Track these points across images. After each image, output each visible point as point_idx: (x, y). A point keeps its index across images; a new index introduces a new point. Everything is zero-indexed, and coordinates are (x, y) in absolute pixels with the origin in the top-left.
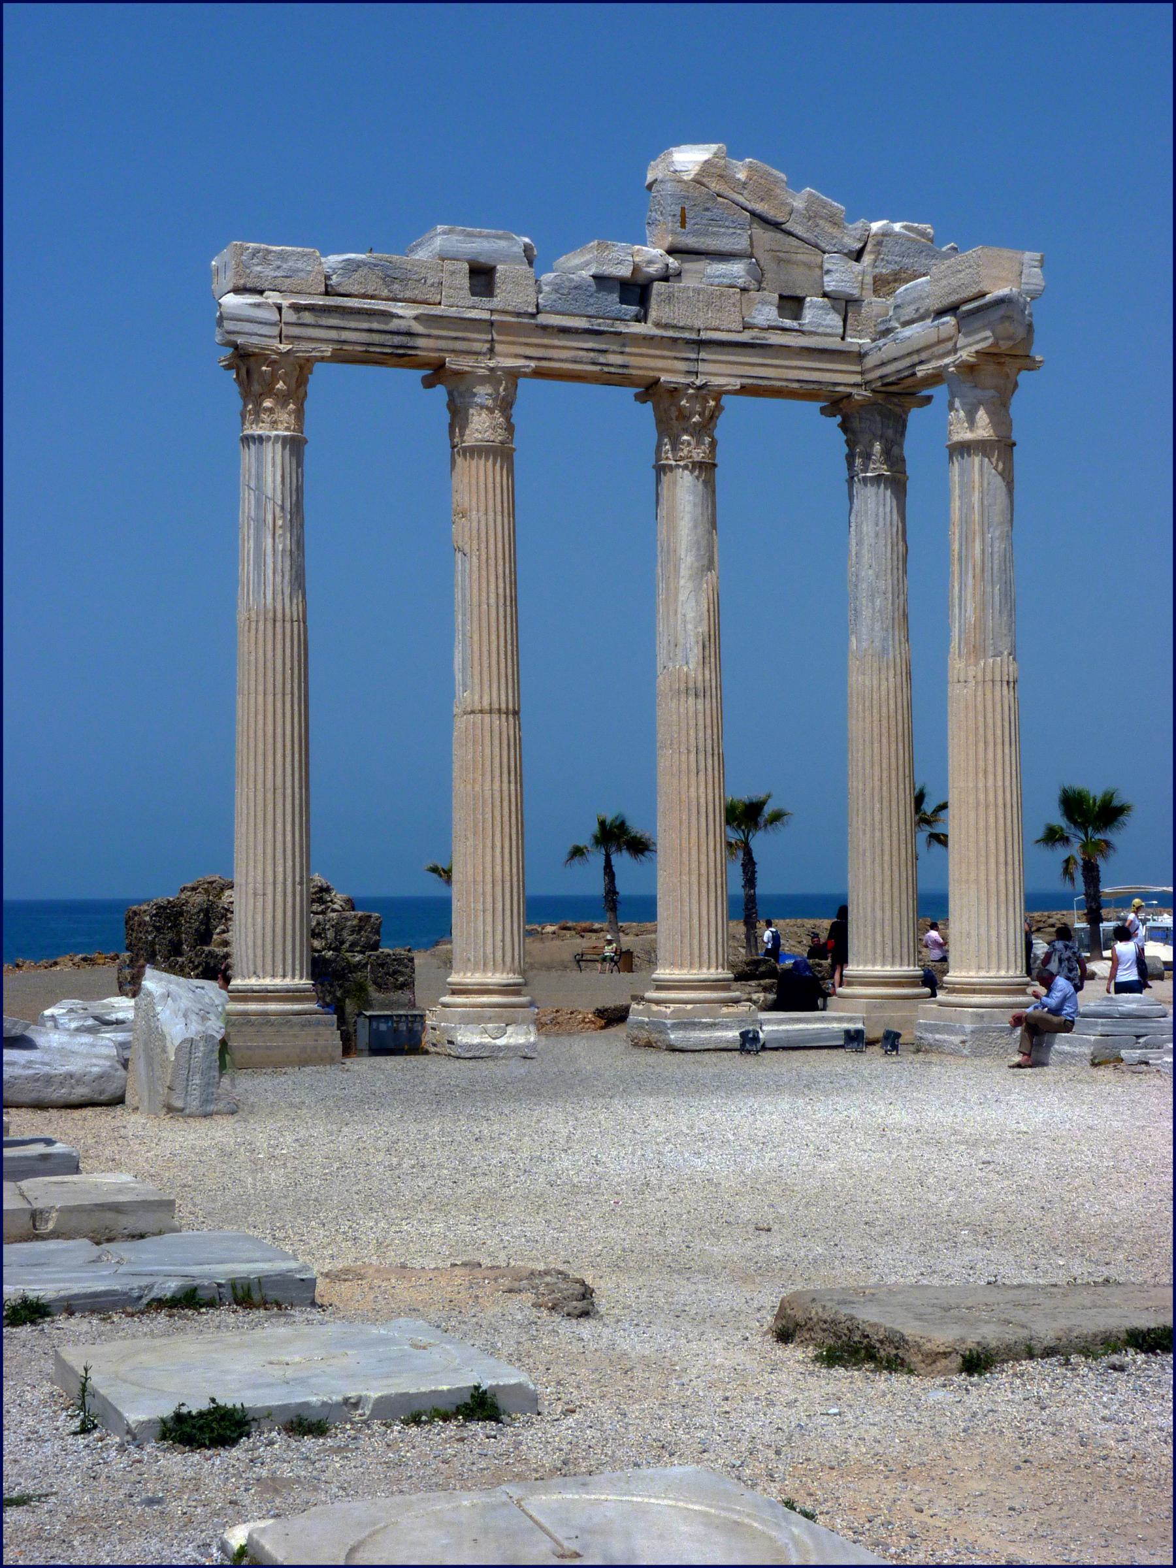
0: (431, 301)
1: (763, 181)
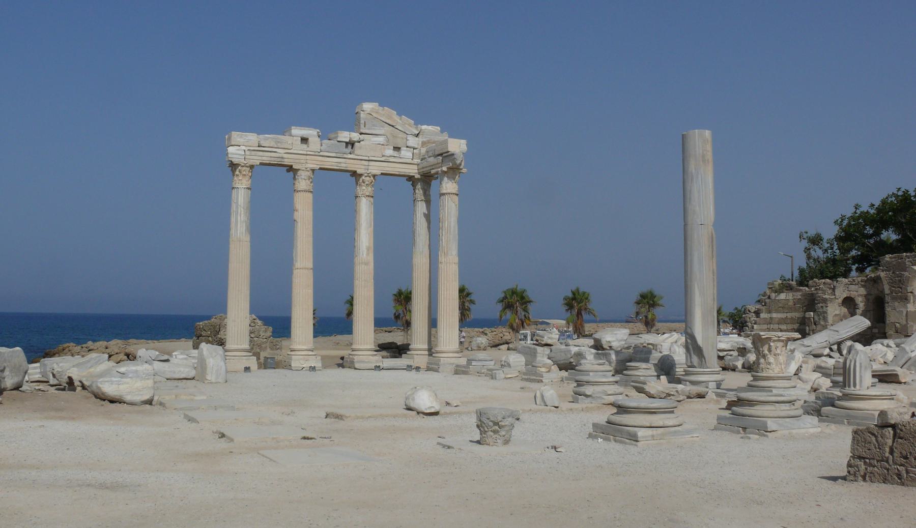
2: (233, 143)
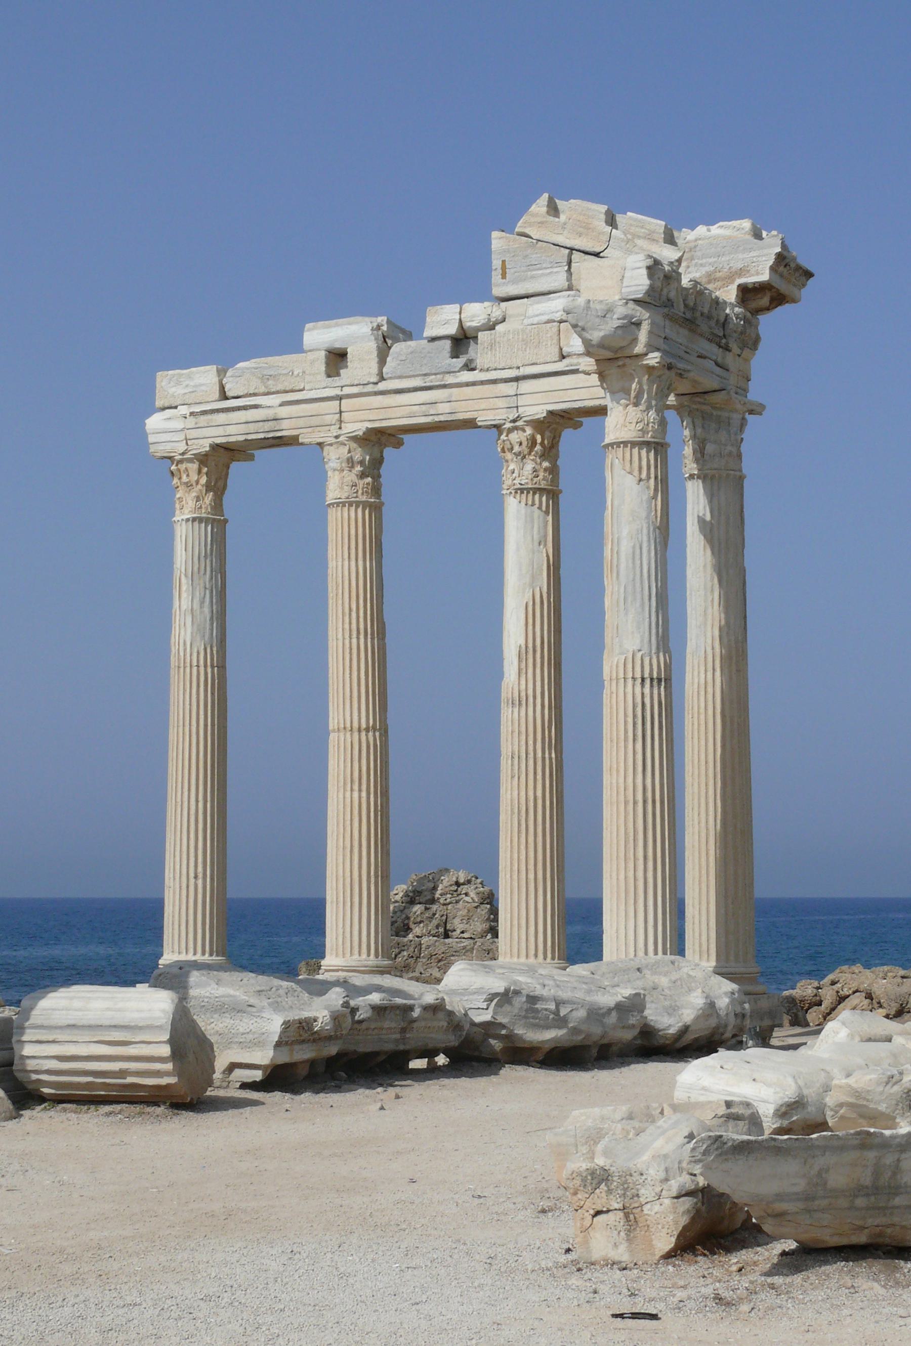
0: (297, 388)
1: (581, 218)
2: (159, 403)
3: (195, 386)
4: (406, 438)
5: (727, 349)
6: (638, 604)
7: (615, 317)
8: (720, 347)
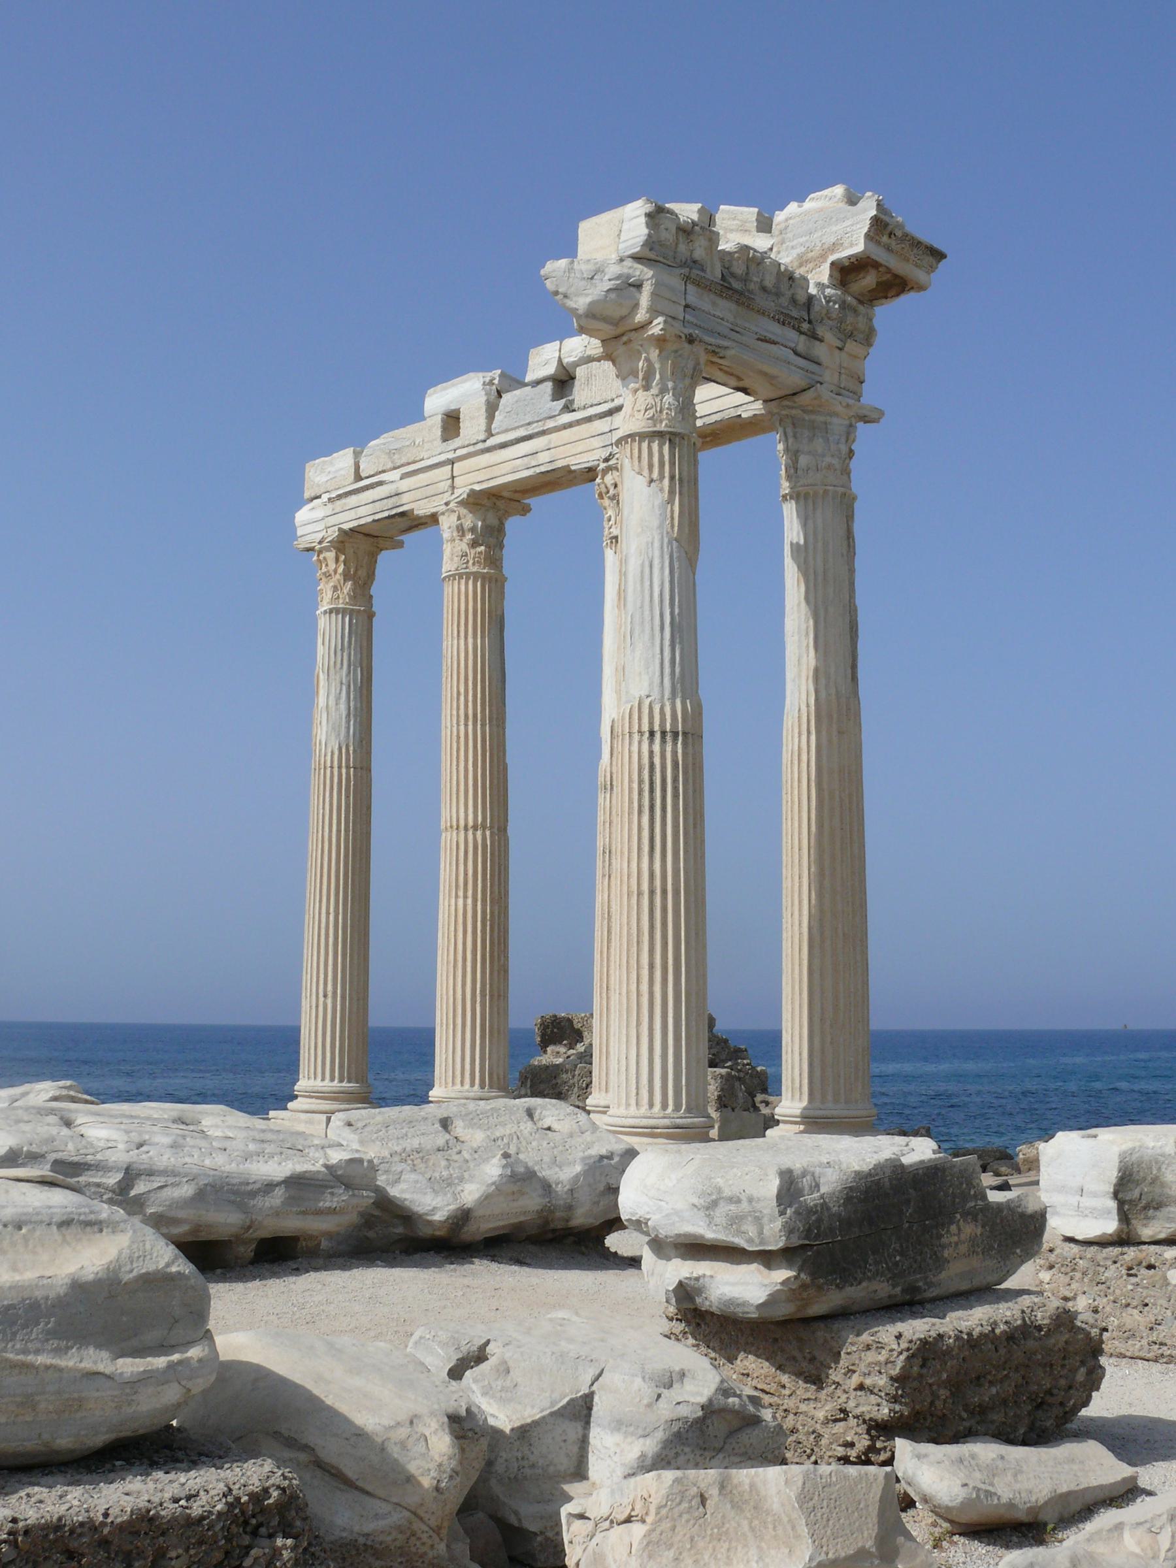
3: (336, 471)
4: (533, 501)
5: (814, 336)
6: (647, 636)
7: (607, 277)
8: (801, 333)
